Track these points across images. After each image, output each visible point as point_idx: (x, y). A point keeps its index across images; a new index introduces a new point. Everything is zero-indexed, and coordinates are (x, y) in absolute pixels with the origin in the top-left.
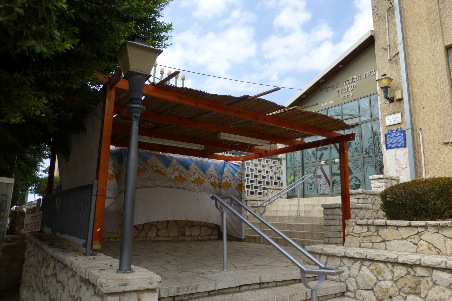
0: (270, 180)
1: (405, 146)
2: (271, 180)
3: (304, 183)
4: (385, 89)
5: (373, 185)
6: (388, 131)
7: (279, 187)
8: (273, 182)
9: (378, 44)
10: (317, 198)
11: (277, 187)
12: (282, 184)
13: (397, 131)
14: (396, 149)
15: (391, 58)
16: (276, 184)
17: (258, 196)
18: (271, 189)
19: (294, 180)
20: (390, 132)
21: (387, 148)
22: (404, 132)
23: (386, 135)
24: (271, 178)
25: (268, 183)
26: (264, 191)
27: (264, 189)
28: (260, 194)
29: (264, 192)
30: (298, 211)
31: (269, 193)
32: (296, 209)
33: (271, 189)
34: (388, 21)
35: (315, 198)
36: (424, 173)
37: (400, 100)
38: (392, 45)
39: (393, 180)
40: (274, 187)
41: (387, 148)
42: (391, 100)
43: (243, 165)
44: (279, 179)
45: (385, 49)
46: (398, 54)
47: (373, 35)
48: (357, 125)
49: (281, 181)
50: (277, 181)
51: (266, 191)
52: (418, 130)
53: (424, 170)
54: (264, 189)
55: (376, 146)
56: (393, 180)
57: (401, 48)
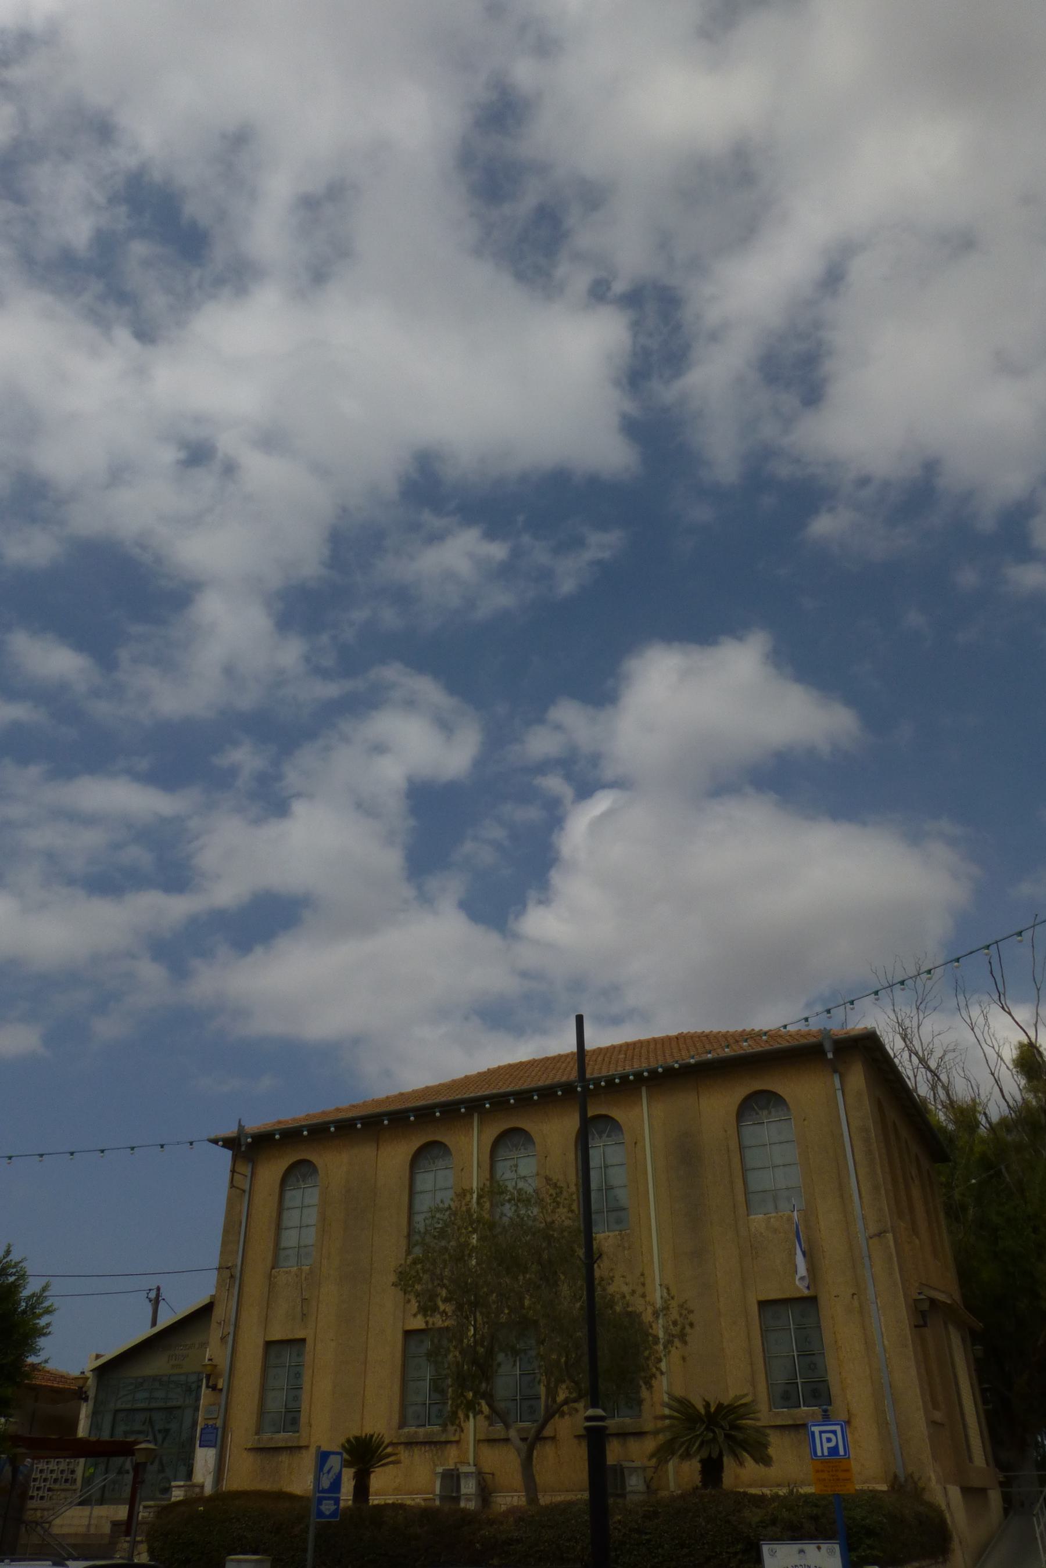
0: (60, 1476)
1: (214, 1446)
2: (61, 1475)
3: (104, 1486)
4: (208, 1377)
5: (174, 1493)
6: (205, 1425)
7: (71, 1485)
8: (64, 1478)
9: (218, 1313)
10: (115, 1506)
11: (68, 1486)
12: (75, 1480)
13: (212, 1425)
14: (207, 1448)
15: (224, 1336)
16: (66, 1481)
17: (39, 1501)
18: (57, 1490)
19: (93, 1474)
20: (206, 1426)
21: (200, 1446)
22: (217, 1429)
23: (202, 1429)
24: (62, 1472)
25: (56, 1481)
26: (49, 1493)
27: (49, 1490)
28: (42, 1498)
29: (48, 1495)
30: (89, 1525)
31: (54, 1497)
32: (87, 1523)
33: (57, 1490)
34: (228, 1290)
35: (113, 1506)
36: (225, 1480)
37: (221, 1390)
38: (226, 1320)
39: (196, 1486)
40: (64, 1486)
41: (200, 1446)
42: (214, 1388)
43: (32, 1465)
44: (73, 1472)
45: (220, 1323)
46: (229, 1334)
47: (212, 1300)
48: (179, 1407)
49: (74, 1476)
50: (70, 1476)
51: (50, 1493)
52: (229, 1429)
53: (225, 1477)
54: (49, 1490)
55: (192, 1440)
56: (196, 1486)
57: (232, 1328)
